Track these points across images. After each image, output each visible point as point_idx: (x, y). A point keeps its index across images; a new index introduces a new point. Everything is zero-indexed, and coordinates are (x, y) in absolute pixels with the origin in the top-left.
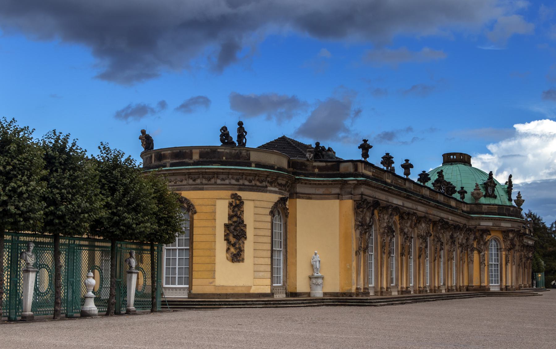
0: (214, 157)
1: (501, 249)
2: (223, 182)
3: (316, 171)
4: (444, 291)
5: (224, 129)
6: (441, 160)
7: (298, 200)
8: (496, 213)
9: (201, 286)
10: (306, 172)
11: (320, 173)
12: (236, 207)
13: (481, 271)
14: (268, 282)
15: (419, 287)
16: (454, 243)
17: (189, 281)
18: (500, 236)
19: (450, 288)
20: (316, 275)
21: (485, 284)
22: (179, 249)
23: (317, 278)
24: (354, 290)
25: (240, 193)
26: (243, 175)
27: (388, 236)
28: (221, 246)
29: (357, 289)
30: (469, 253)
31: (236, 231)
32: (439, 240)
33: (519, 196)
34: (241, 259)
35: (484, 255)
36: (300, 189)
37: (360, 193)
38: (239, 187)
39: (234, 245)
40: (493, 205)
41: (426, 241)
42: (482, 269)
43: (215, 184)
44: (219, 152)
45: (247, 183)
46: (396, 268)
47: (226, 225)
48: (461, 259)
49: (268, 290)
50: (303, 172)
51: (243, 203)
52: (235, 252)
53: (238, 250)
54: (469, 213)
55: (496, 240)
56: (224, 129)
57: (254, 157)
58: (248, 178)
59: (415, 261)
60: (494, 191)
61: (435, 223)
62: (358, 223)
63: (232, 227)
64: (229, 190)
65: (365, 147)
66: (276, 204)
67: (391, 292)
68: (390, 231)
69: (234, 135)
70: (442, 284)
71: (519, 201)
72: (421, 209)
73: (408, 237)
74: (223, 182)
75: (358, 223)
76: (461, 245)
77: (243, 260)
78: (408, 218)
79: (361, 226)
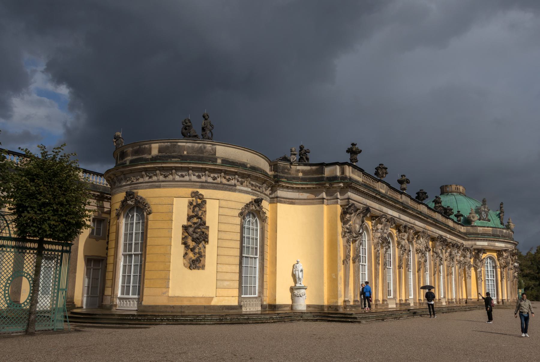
0: (174, 152)
2: (182, 179)
3: (300, 175)
4: (444, 304)
7: (278, 204)
9: (153, 297)
10: (289, 176)
11: (304, 177)
12: (197, 207)
14: (236, 292)
15: (419, 300)
16: (453, 260)
17: (140, 291)
18: (495, 255)
19: (450, 301)
20: (298, 285)
22: (135, 255)
23: (300, 288)
24: (340, 302)
25: (202, 191)
27: (382, 247)
28: (177, 250)
29: (345, 301)
30: (467, 269)
31: (196, 233)
34: (201, 265)
35: (480, 272)
36: (280, 193)
38: (200, 184)
39: (192, 250)
41: (425, 255)
42: (479, 284)
43: (174, 181)
44: (179, 146)
45: (210, 180)
46: (393, 280)
47: (185, 228)
48: (460, 274)
49: (234, 302)
50: (286, 175)
51: (205, 202)
52: (194, 258)
53: (198, 255)
55: (491, 258)
58: (212, 175)
59: (414, 274)
60: (487, 215)
61: (433, 239)
63: (191, 230)
64: (189, 187)
65: (353, 151)
66: (247, 205)
67: (387, 304)
68: (385, 242)
70: (442, 297)
72: (419, 225)
73: (405, 250)
74: (182, 179)
75: (346, 230)
76: (459, 262)
77: (203, 267)
79: (349, 232)
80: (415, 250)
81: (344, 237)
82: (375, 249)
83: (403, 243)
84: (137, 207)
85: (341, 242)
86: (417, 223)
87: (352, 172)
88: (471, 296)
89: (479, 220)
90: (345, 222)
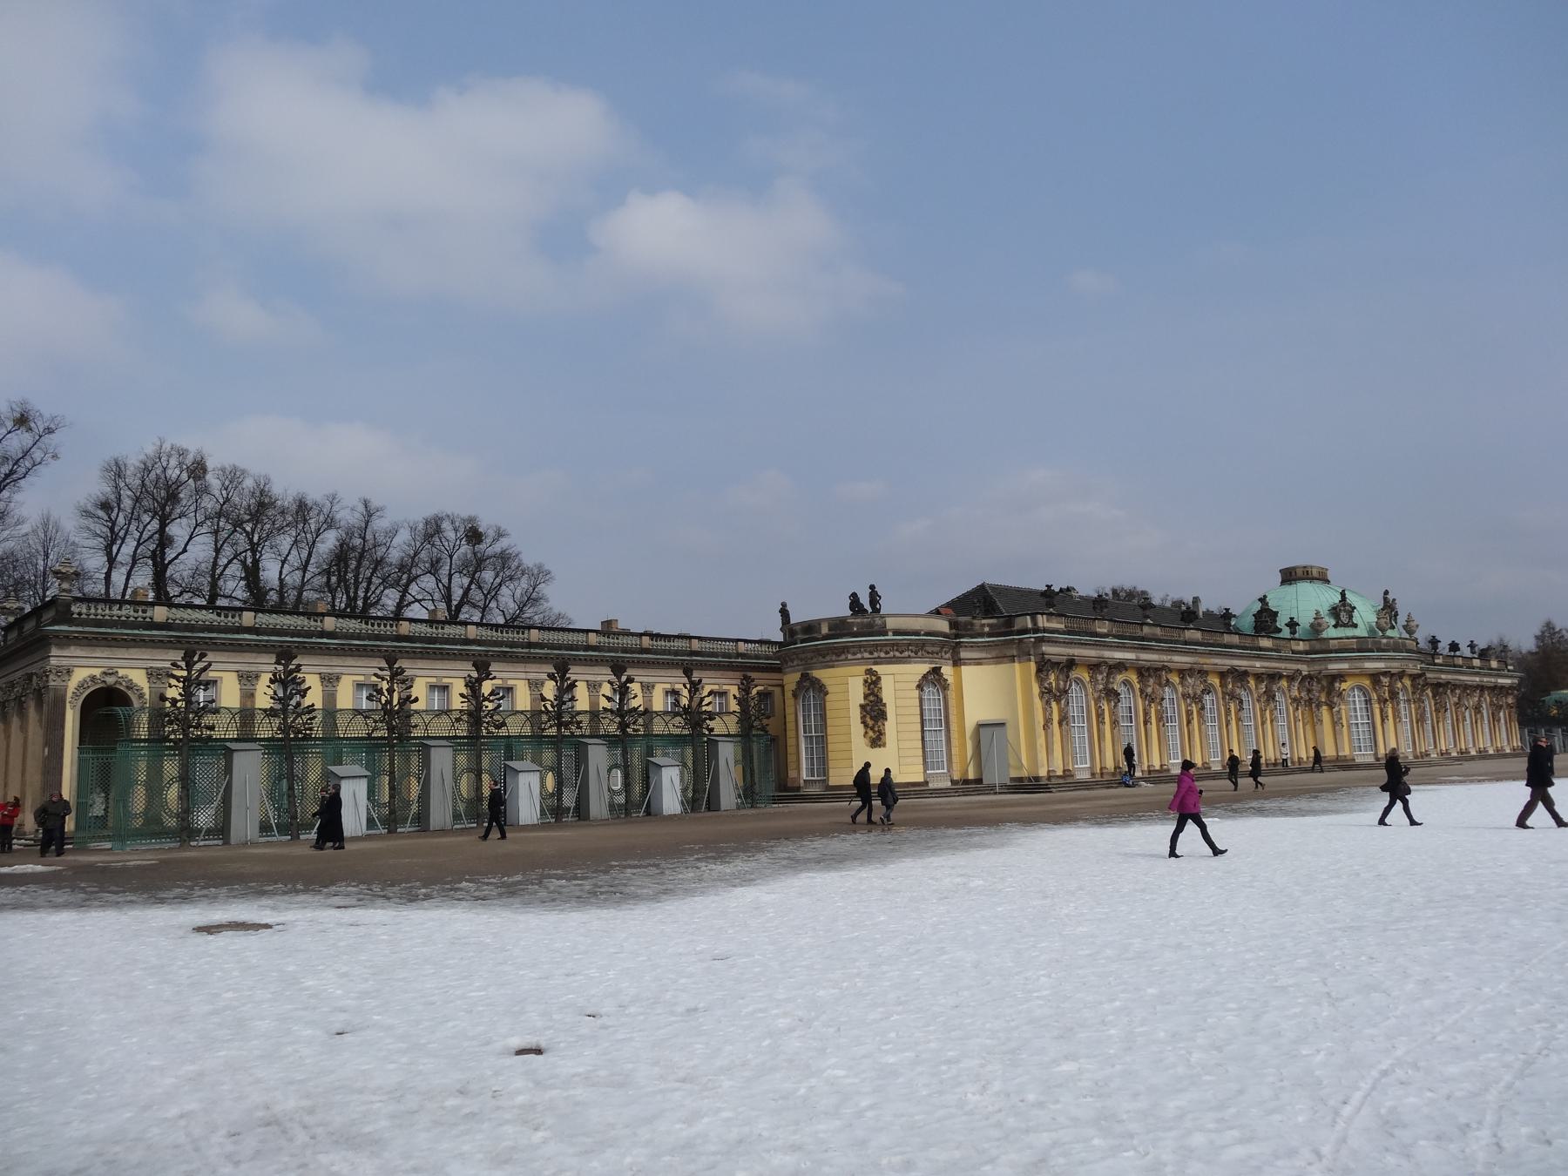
5: (854, 595)
12: (873, 684)
17: (824, 771)
18: (1367, 683)
21: (1346, 752)
24: (1043, 773)
25: (875, 668)
26: (876, 647)
27: (1109, 701)
28: (857, 729)
31: (874, 712)
32: (1233, 696)
54: (1307, 653)
55: (1360, 688)
56: (854, 595)
57: (891, 623)
60: (1351, 617)
61: (1223, 675)
66: (925, 677)
69: (865, 601)
77: (884, 745)
81: (1041, 698)
83: (1149, 690)
84: (812, 688)
85: (1038, 704)
86: (1176, 658)
90: (1041, 681)
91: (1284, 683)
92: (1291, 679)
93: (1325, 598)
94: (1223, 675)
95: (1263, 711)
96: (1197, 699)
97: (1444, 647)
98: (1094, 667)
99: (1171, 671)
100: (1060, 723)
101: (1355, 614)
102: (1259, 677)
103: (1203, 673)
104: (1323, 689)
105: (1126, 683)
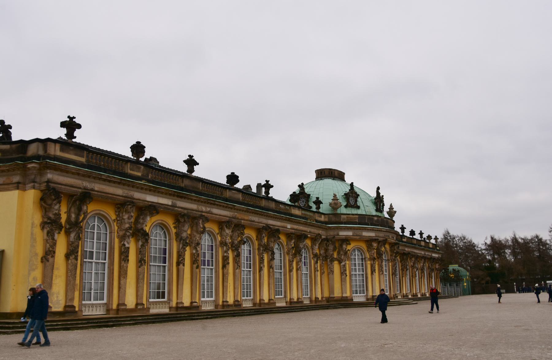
1: (365, 258)
6: (314, 176)
8: (356, 222)
13: (343, 281)
15: (223, 302)
16: (299, 253)
18: (363, 246)
21: (348, 294)
27: (137, 241)
33: (391, 208)
35: (345, 266)
37: (46, 180)
40: (353, 215)
54: (326, 223)
55: (359, 250)
60: (356, 201)
62: (46, 220)
71: (392, 213)
78: (185, 221)
79: (49, 223)
80: (218, 243)
82: (120, 242)
83: (184, 235)
86: (215, 211)
87: (62, 150)
88: (334, 294)
89: (346, 207)
91: (308, 242)
92: (314, 240)
93: (340, 189)
94: (259, 231)
95: (291, 262)
96: (236, 248)
97: (407, 233)
98: (121, 205)
99: (207, 220)
100: (67, 257)
101: (359, 199)
102: (289, 236)
103: (239, 227)
104: (334, 250)
105: (163, 226)
